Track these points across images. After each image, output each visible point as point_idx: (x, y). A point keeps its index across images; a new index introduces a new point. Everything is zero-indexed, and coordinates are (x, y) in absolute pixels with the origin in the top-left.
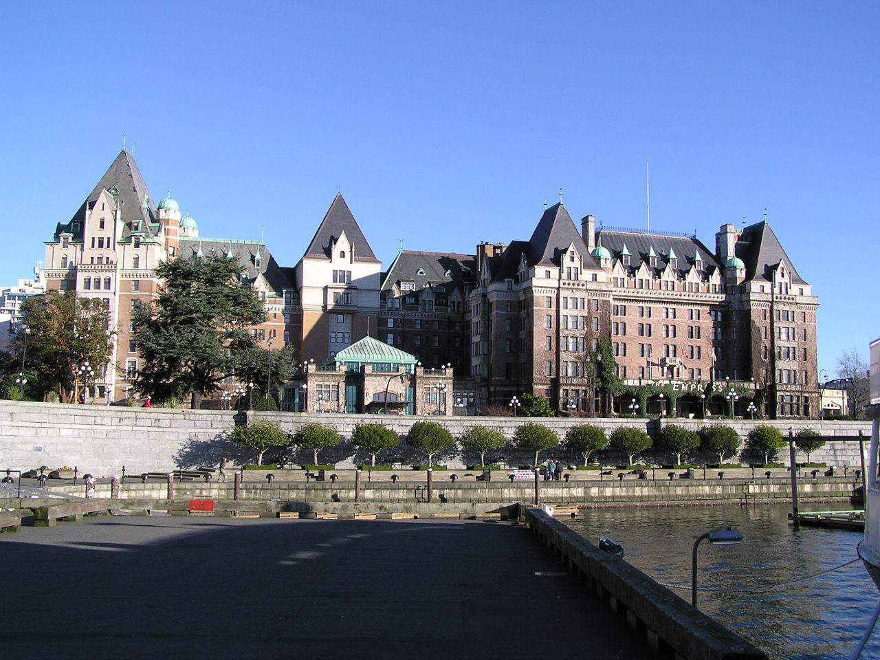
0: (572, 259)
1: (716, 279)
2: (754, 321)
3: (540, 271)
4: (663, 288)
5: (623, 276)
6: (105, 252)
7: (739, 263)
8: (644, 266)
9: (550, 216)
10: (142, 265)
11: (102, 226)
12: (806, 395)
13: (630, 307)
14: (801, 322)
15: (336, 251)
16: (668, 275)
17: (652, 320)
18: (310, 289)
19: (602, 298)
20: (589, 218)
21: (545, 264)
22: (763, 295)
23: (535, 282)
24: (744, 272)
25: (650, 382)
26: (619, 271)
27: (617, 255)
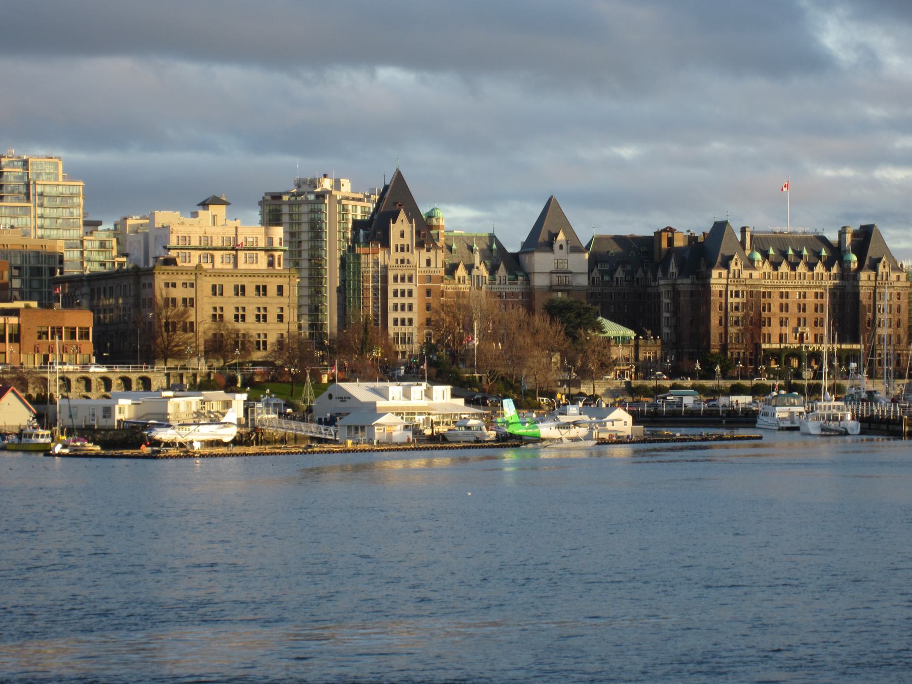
0: (736, 264)
1: (835, 270)
2: (861, 301)
3: (715, 273)
4: (797, 278)
5: (770, 271)
6: (406, 255)
7: (854, 258)
8: (784, 263)
9: (720, 228)
10: (433, 264)
11: (402, 236)
12: (899, 352)
13: (774, 292)
14: (896, 300)
15: (556, 246)
16: (801, 268)
17: (789, 301)
18: (539, 274)
19: (755, 290)
20: (747, 229)
21: (718, 268)
22: (869, 282)
23: (712, 281)
24: (856, 264)
25: (787, 345)
26: (767, 268)
27: (765, 255)
